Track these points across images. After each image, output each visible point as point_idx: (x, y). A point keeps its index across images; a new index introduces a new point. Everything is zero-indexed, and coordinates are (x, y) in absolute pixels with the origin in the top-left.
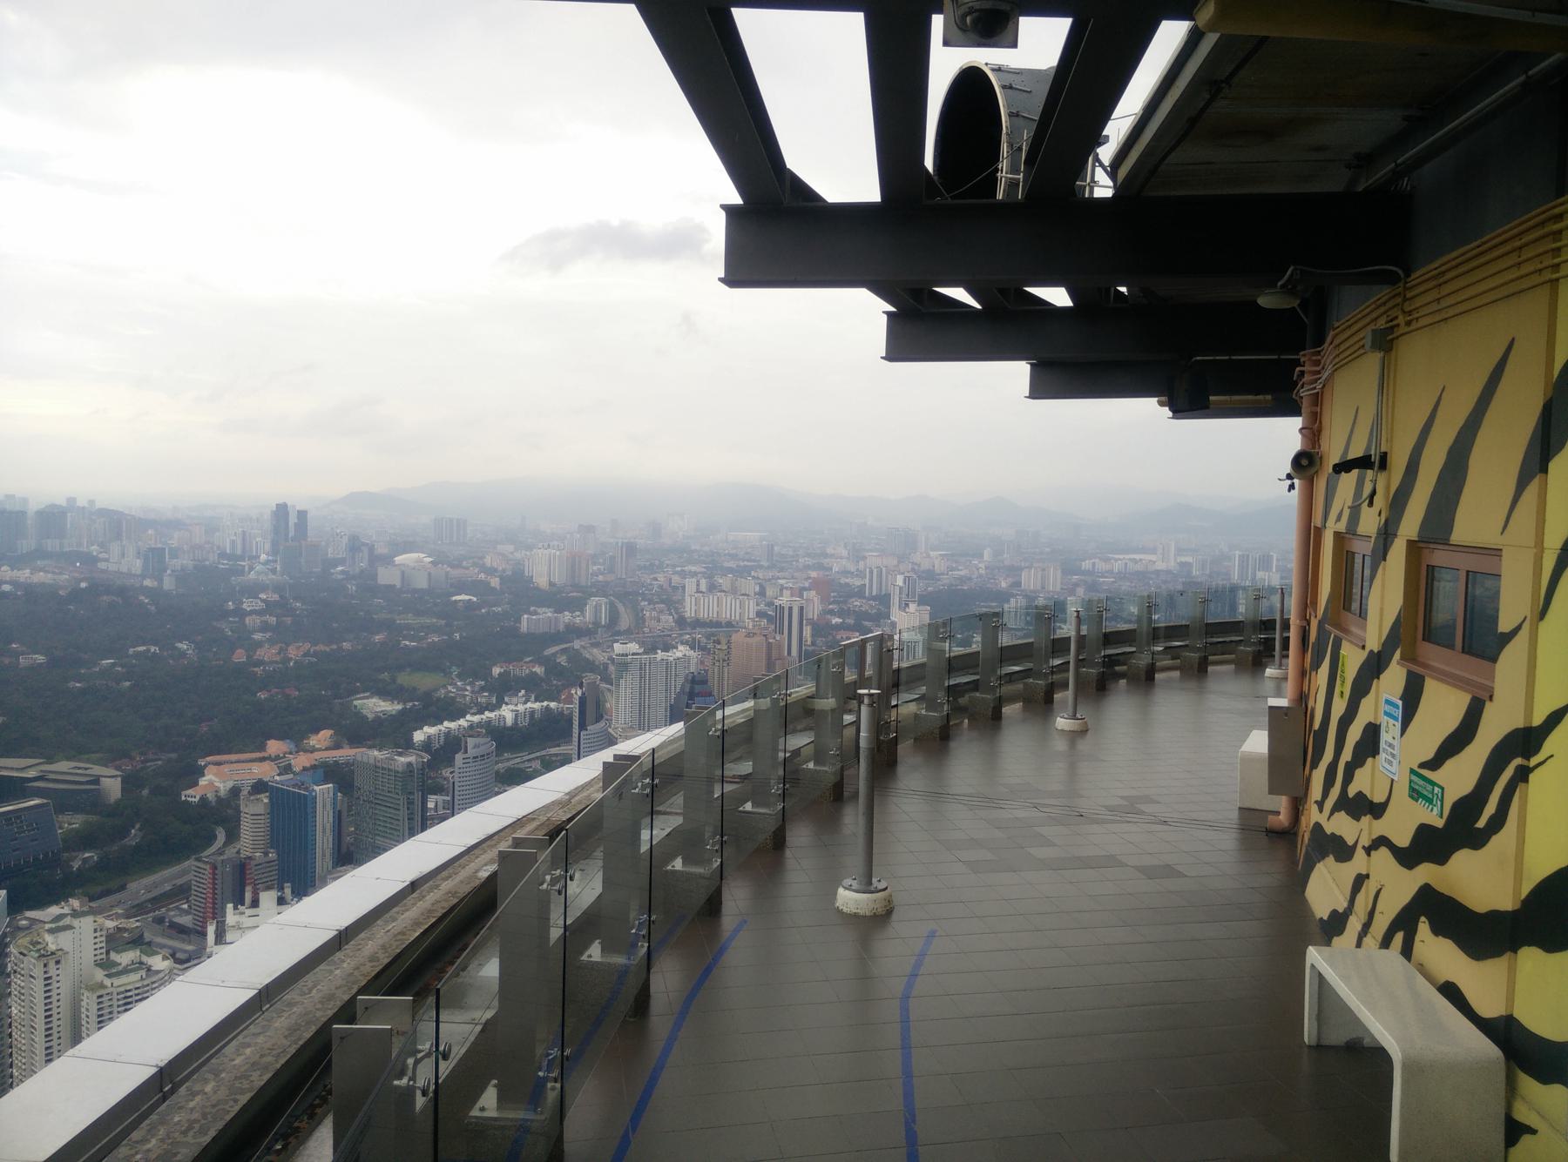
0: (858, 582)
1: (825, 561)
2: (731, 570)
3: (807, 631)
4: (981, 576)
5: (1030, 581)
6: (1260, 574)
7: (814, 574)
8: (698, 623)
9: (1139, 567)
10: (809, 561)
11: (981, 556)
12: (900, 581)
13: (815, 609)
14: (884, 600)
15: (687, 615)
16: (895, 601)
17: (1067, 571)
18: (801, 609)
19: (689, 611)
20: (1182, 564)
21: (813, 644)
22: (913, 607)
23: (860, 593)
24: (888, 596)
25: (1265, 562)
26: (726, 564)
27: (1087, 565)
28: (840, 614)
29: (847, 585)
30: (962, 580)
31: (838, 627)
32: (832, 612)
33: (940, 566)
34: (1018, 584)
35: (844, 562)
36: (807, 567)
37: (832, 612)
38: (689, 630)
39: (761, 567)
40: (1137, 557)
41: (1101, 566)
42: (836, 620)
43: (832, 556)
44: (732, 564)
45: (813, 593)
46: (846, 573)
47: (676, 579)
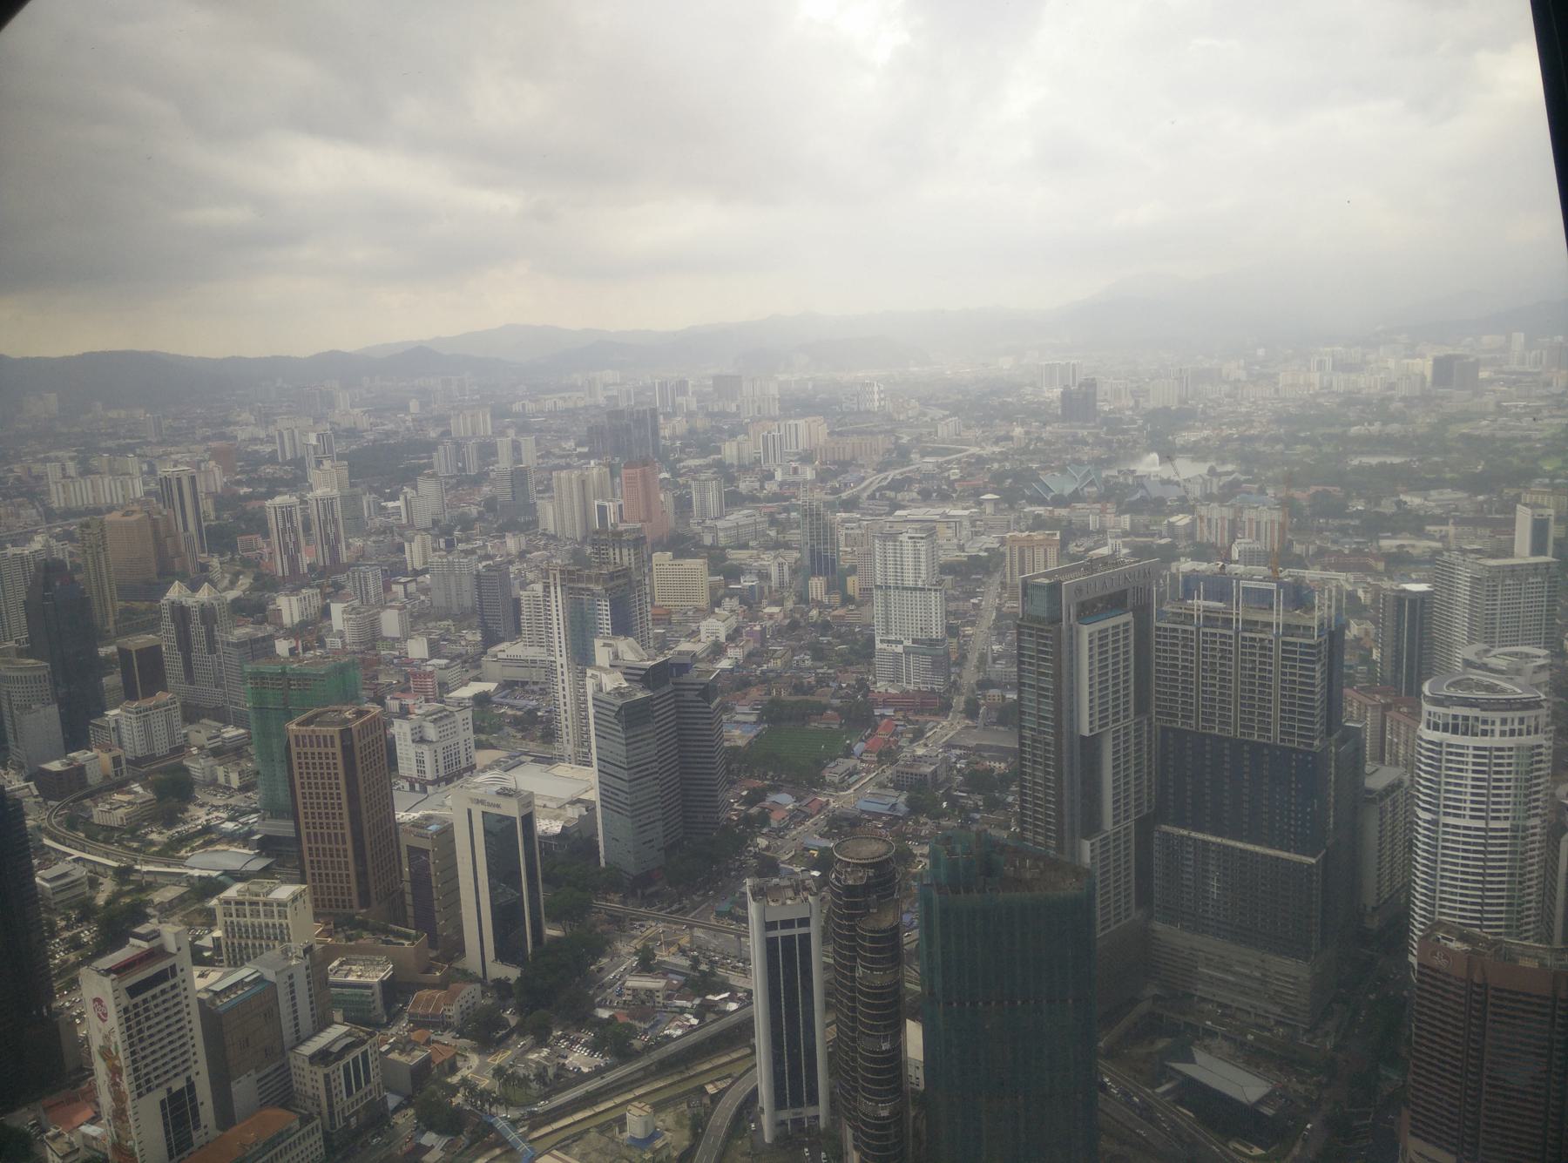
0: (268, 449)
1: (228, 430)
2: (108, 450)
3: (207, 506)
4: (408, 429)
5: (460, 426)
6: (679, 399)
7: (213, 444)
8: (68, 513)
9: (571, 405)
10: (209, 432)
11: (406, 409)
12: (313, 439)
13: (216, 478)
14: (299, 463)
15: (55, 505)
16: (311, 461)
17: (499, 413)
18: (193, 479)
19: (57, 501)
20: (609, 398)
21: (217, 518)
22: (327, 464)
23: (272, 459)
24: (303, 458)
25: (681, 387)
26: (103, 444)
27: (517, 407)
28: (248, 484)
29: (257, 452)
30: (387, 434)
31: (247, 498)
32: (239, 483)
33: (364, 422)
34: (447, 433)
35: (250, 428)
36: (206, 439)
37: (239, 483)
38: (59, 522)
39: (148, 443)
40: (566, 395)
41: (530, 407)
42: (244, 490)
43: (236, 423)
44: (111, 444)
45: (212, 463)
46: (254, 440)
47: (37, 468)
